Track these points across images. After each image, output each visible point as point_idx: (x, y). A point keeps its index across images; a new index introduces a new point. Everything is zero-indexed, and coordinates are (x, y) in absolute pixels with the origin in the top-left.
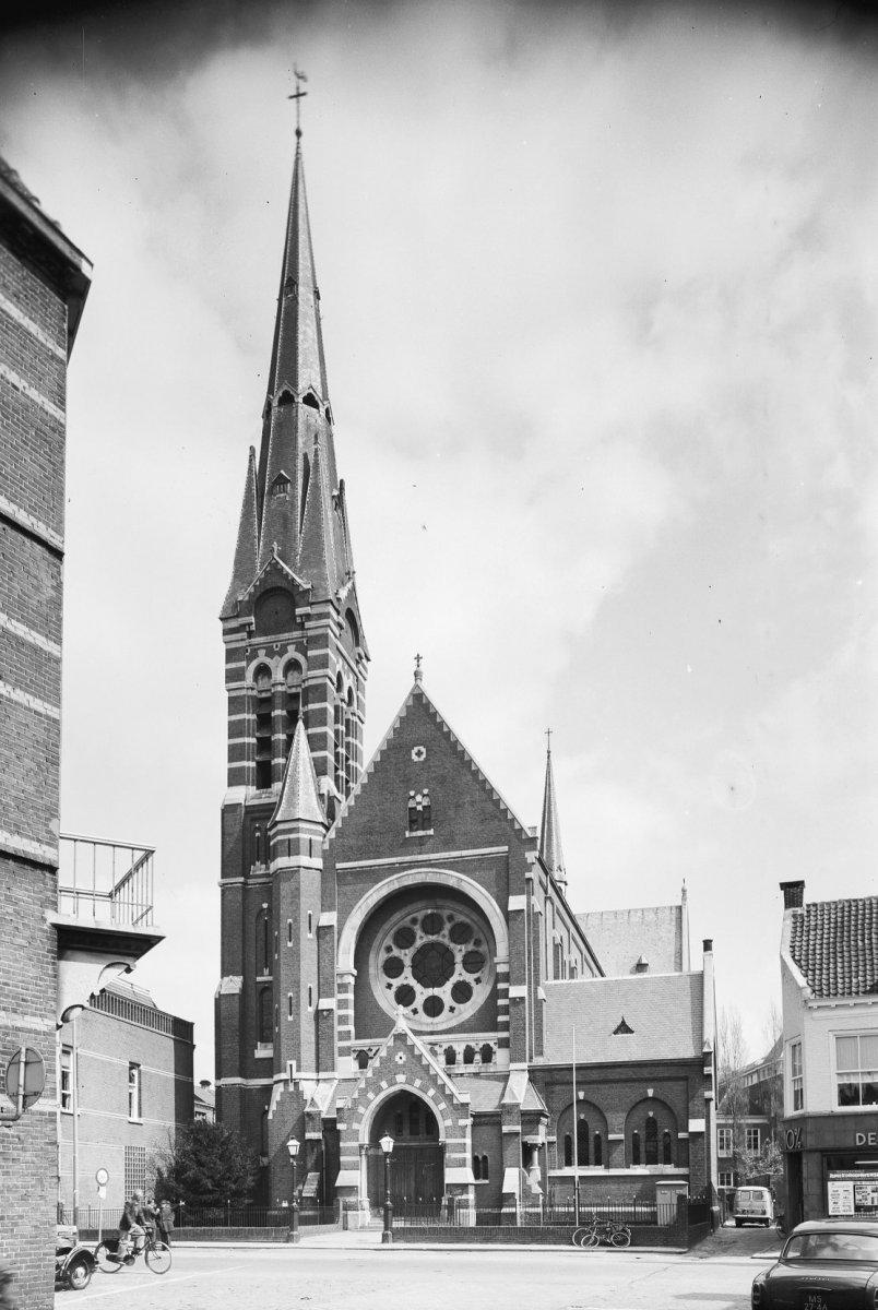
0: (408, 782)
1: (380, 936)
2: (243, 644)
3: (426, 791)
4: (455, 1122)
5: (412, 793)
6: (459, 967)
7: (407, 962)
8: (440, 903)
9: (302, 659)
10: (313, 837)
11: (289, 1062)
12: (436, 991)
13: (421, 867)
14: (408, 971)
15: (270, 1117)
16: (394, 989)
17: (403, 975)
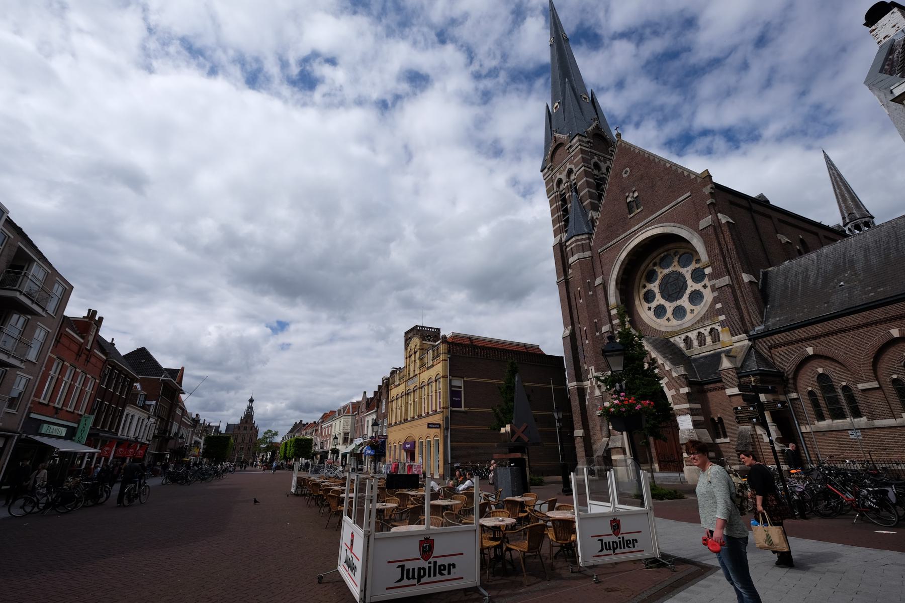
0: (623, 190)
1: (637, 280)
2: (551, 176)
3: (634, 189)
4: (677, 391)
5: (627, 194)
6: (690, 282)
7: (656, 290)
8: (666, 247)
9: (573, 167)
10: (583, 242)
11: (590, 368)
12: (679, 303)
13: (642, 230)
14: (658, 296)
15: (587, 403)
16: (652, 310)
17: (656, 300)
